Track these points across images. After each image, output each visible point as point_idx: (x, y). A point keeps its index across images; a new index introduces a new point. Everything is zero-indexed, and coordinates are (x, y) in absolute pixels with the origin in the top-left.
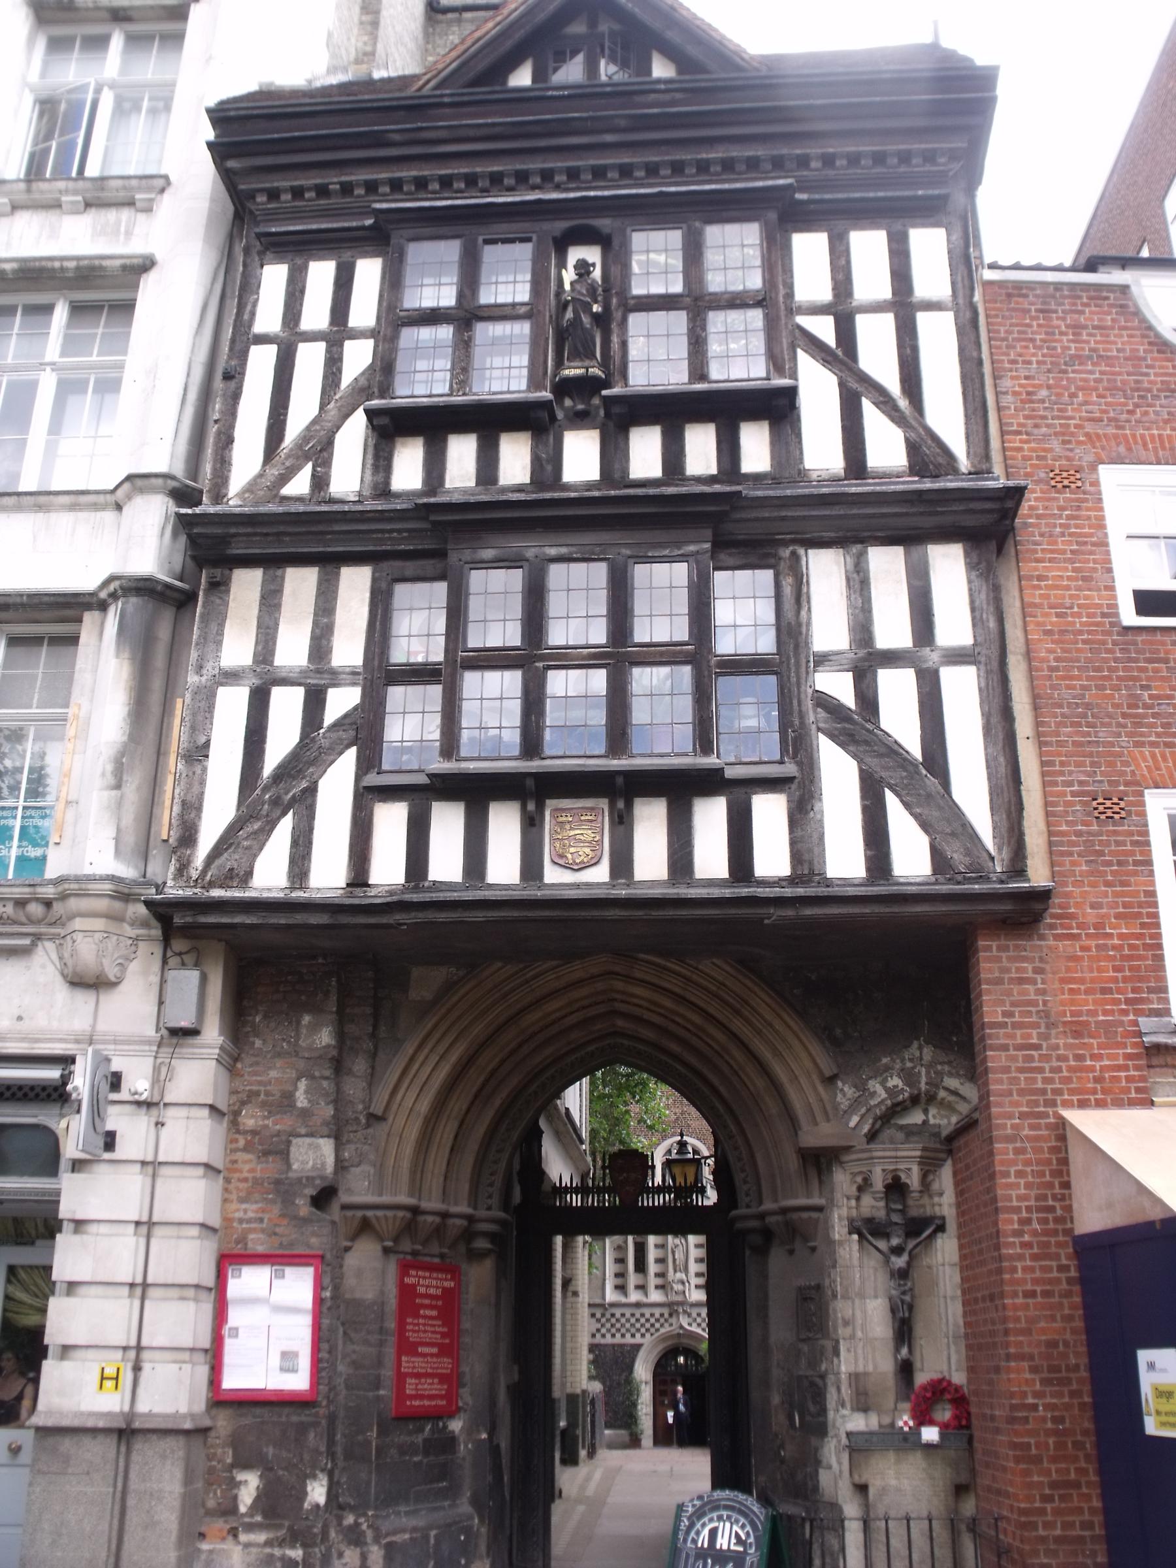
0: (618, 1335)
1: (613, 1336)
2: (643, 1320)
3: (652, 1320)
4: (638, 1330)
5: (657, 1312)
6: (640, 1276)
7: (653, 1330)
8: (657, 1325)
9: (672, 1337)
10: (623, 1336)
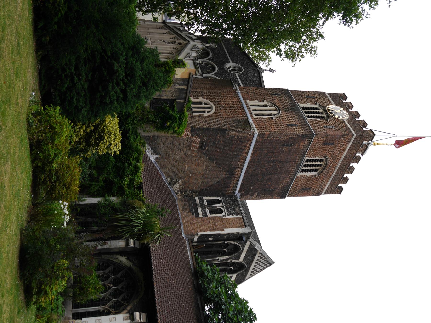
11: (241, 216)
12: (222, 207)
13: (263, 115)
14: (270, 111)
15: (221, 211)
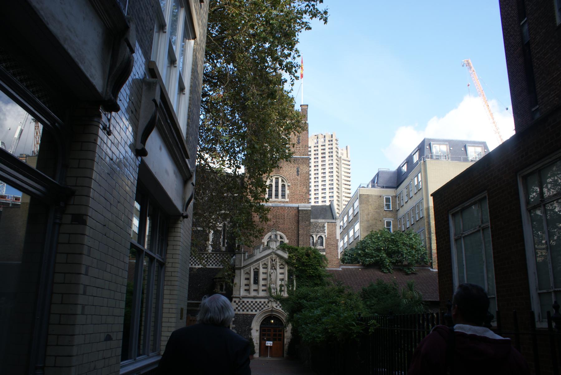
0: (245, 310)
1: (243, 310)
2: (256, 304)
3: (260, 304)
4: (254, 308)
5: (263, 300)
6: (256, 285)
7: (260, 309)
8: (262, 307)
9: (268, 312)
10: (247, 311)
11: (326, 223)
12: (316, 235)
13: (283, 191)
14: (277, 183)
15: (321, 237)
